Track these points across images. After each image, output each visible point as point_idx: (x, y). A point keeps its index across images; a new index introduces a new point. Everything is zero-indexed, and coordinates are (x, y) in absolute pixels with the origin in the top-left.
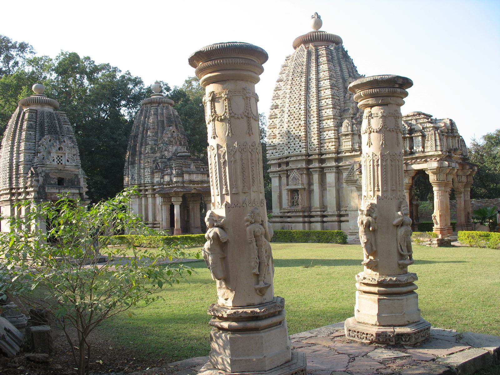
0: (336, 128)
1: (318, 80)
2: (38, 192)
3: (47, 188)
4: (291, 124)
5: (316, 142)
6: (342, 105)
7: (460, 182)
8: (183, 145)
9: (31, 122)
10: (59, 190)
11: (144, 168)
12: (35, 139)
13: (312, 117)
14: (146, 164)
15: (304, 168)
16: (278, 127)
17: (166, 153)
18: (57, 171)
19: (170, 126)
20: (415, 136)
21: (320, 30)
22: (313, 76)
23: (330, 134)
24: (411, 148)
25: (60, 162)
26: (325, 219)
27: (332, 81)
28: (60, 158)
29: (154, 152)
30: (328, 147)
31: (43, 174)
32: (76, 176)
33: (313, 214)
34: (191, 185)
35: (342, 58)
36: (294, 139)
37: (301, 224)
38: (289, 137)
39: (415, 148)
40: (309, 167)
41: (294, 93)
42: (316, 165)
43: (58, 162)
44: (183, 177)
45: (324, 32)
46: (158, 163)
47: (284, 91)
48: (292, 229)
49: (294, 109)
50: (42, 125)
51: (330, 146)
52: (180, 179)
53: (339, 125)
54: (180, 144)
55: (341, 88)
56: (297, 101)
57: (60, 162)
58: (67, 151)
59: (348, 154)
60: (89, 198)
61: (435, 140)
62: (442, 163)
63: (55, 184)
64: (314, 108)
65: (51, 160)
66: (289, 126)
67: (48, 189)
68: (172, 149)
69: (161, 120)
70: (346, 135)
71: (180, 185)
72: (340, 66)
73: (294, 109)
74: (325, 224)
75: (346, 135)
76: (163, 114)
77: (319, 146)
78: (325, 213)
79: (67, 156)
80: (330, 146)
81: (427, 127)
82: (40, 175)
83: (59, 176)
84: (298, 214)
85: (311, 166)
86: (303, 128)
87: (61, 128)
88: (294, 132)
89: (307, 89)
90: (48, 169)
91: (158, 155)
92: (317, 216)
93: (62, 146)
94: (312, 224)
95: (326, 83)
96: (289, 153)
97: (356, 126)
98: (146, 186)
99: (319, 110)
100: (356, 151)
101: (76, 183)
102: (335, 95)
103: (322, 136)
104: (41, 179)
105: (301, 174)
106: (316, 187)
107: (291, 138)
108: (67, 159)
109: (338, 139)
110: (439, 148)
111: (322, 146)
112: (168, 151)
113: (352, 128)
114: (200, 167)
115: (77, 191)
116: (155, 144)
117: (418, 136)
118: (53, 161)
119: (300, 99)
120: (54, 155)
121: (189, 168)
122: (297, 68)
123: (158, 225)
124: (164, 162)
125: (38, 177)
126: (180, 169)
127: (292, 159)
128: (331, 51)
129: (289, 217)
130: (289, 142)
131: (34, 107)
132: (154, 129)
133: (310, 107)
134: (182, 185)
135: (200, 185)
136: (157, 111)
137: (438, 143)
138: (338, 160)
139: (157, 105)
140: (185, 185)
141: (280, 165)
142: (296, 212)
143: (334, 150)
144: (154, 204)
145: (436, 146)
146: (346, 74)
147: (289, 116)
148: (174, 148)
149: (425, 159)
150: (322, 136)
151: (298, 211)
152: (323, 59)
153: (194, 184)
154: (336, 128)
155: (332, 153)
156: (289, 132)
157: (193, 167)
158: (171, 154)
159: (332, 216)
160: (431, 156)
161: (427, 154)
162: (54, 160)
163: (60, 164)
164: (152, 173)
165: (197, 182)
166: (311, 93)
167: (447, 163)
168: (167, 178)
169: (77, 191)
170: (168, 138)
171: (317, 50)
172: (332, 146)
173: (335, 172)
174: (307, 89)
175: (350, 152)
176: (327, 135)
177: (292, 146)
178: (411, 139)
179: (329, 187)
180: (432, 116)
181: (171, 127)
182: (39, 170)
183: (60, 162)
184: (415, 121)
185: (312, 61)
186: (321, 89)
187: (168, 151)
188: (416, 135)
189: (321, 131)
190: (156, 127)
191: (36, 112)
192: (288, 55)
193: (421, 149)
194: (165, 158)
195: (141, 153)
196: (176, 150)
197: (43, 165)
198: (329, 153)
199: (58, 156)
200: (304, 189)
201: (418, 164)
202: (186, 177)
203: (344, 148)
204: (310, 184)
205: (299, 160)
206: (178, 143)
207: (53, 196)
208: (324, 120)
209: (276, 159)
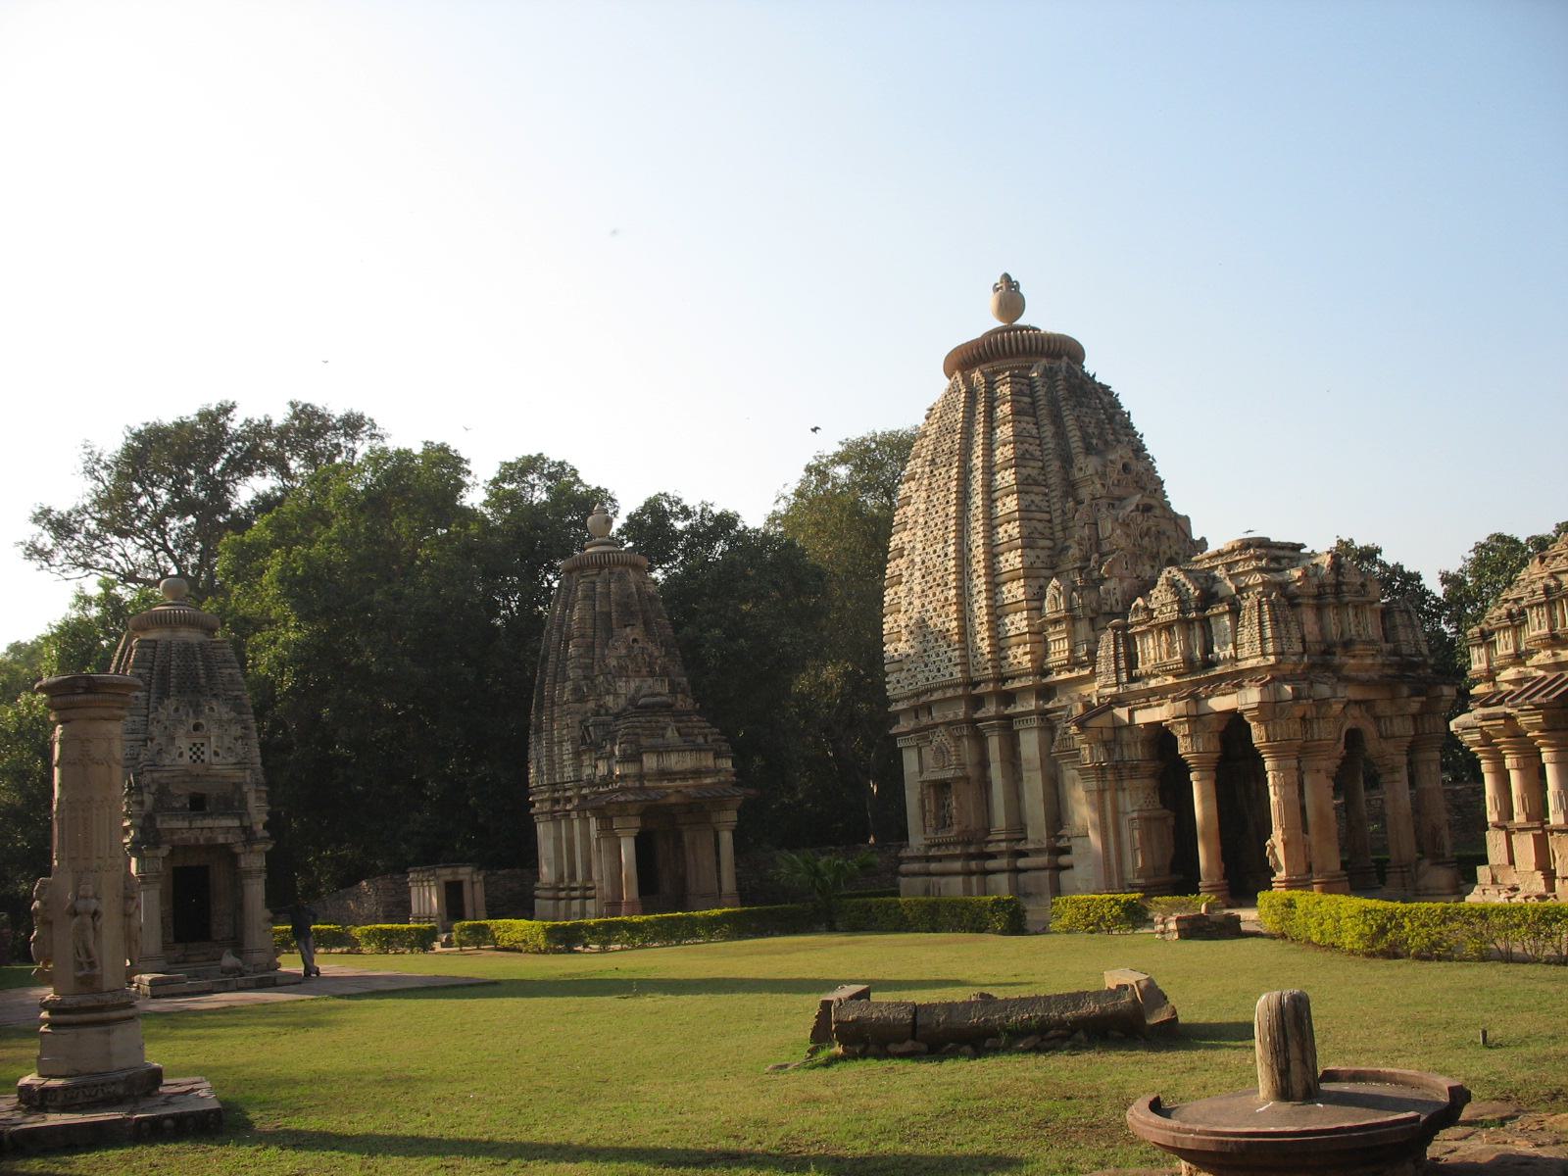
0: (1036, 604)
1: (990, 471)
2: (142, 830)
3: (159, 820)
4: (928, 600)
5: (985, 647)
6: (1059, 534)
7: (1386, 738)
8: (660, 676)
9: (141, 671)
10: (190, 822)
11: (560, 743)
12: (148, 708)
13: (974, 576)
14: (565, 732)
15: (960, 722)
16: (903, 609)
17: (609, 700)
18: (187, 779)
19: (626, 626)
20: (1216, 615)
21: (1021, 322)
22: (977, 461)
23: (1017, 623)
24: (1208, 649)
25: (199, 757)
26: (1021, 863)
27: (1023, 471)
28: (198, 749)
29: (582, 699)
30: (1015, 657)
31: (153, 788)
32: (238, 787)
33: (992, 848)
34: (665, 783)
35: (1065, 399)
36: (937, 640)
37: (960, 879)
38: (925, 636)
39: (1216, 649)
40: (976, 716)
41: (933, 511)
42: (991, 709)
43: (194, 757)
44: (641, 761)
45: (1034, 329)
46: (587, 728)
47: (916, 506)
48: (940, 895)
49: (934, 556)
50: (164, 674)
51: (1020, 657)
52: (631, 769)
53: (1037, 597)
54: (652, 674)
55: (1053, 487)
56: (941, 533)
57: (199, 757)
58: (215, 731)
59: (1064, 676)
60: (271, 838)
61: (1261, 623)
62: (1278, 691)
63: (183, 808)
64: (979, 553)
65: (175, 752)
66: (923, 606)
67: (162, 822)
68: (626, 687)
69: (602, 612)
70: (1056, 622)
71: (630, 784)
72: (1057, 419)
73: (934, 556)
74: (1022, 877)
75: (1056, 622)
76: (608, 595)
77: (995, 656)
78: (1021, 846)
79: (213, 745)
80: (1020, 657)
81: (1247, 587)
82: (146, 790)
83: (193, 790)
84: (952, 851)
85: (978, 715)
86: (954, 608)
87: (210, 676)
88: (936, 623)
89: (964, 497)
90: (166, 774)
91: (591, 705)
92: (1001, 853)
93: (201, 721)
94: (991, 877)
95: (1006, 478)
96: (927, 679)
97: (1080, 596)
98: (565, 790)
99: (992, 554)
100: (1082, 665)
101: (236, 804)
102: (1033, 508)
103: (1001, 629)
104: (148, 799)
105: (959, 738)
106: (996, 772)
107: (929, 637)
108: (213, 747)
109: (1038, 637)
110: (1270, 648)
111: (1002, 655)
112: (616, 695)
113: (1069, 601)
114: (696, 731)
115: (236, 823)
116: (586, 678)
117: (1222, 614)
118: (180, 754)
119: (946, 528)
120: (183, 743)
121: (663, 736)
122: (942, 439)
123: (593, 892)
124: (603, 724)
125: (142, 795)
126: (632, 742)
127: (937, 696)
128: (1031, 383)
129: (939, 859)
130: (925, 651)
131: (152, 635)
132: (582, 636)
133: (971, 550)
134: (637, 784)
135: (691, 782)
136: (594, 589)
137: (1268, 633)
138: (1046, 692)
139: (595, 572)
140: (646, 784)
141: (916, 711)
142: (947, 844)
143: (960, 675)
144: (586, 835)
145: (1263, 640)
146: (1075, 445)
147: (923, 577)
148: (633, 685)
149: (1237, 680)
150: (1001, 629)
151: (951, 843)
152: (1004, 410)
153: (675, 780)
154: (1036, 604)
155: (1027, 675)
156: (924, 621)
157: (671, 734)
158: (622, 701)
159: (1038, 852)
160: (1253, 670)
161: (1243, 665)
162: (181, 755)
163: (199, 761)
164: (577, 755)
165: (683, 775)
166: (973, 507)
167: (1288, 688)
168: (602, 769)
169: (236, 823)
170: (619, 658)
171: (991, 386)
172: (1025, 654)
173: (1040, 729)
174: (964, 497)
175: (1070, 671)
176: (1012, 623)
177: (932, 659)
178: (1206, 624)
179: (1028, 770)
180: (1302, 546)
181: (628, 630)
182: (146, 779)
183: (198, 757)
184: (1224, 571)
185: (978, 417)
186: (997, 494)
187: (616, 695)
188: (1215, 611)
189: (997, 612)
190: (590, 632)
191: (153, 644)
192: (930, 405)
193: (1229, 650)
194: (607, 714)
195: (553, 703)
196: (638, 689)
197: (154, 765)
198: (1020, 676)
199: (195, 745)
200: (966, 779)
201: (1223, 695)
202: (650, 762)
203: (1052, 658)
204: (984, 764)
205: (950, 699)
206: (644, 671)
207: (175, 837)
208: (1005, 583)
209: (908, 698)
